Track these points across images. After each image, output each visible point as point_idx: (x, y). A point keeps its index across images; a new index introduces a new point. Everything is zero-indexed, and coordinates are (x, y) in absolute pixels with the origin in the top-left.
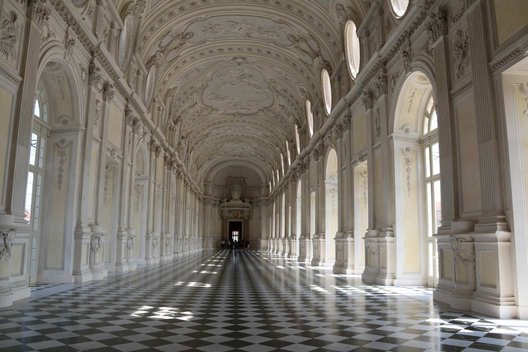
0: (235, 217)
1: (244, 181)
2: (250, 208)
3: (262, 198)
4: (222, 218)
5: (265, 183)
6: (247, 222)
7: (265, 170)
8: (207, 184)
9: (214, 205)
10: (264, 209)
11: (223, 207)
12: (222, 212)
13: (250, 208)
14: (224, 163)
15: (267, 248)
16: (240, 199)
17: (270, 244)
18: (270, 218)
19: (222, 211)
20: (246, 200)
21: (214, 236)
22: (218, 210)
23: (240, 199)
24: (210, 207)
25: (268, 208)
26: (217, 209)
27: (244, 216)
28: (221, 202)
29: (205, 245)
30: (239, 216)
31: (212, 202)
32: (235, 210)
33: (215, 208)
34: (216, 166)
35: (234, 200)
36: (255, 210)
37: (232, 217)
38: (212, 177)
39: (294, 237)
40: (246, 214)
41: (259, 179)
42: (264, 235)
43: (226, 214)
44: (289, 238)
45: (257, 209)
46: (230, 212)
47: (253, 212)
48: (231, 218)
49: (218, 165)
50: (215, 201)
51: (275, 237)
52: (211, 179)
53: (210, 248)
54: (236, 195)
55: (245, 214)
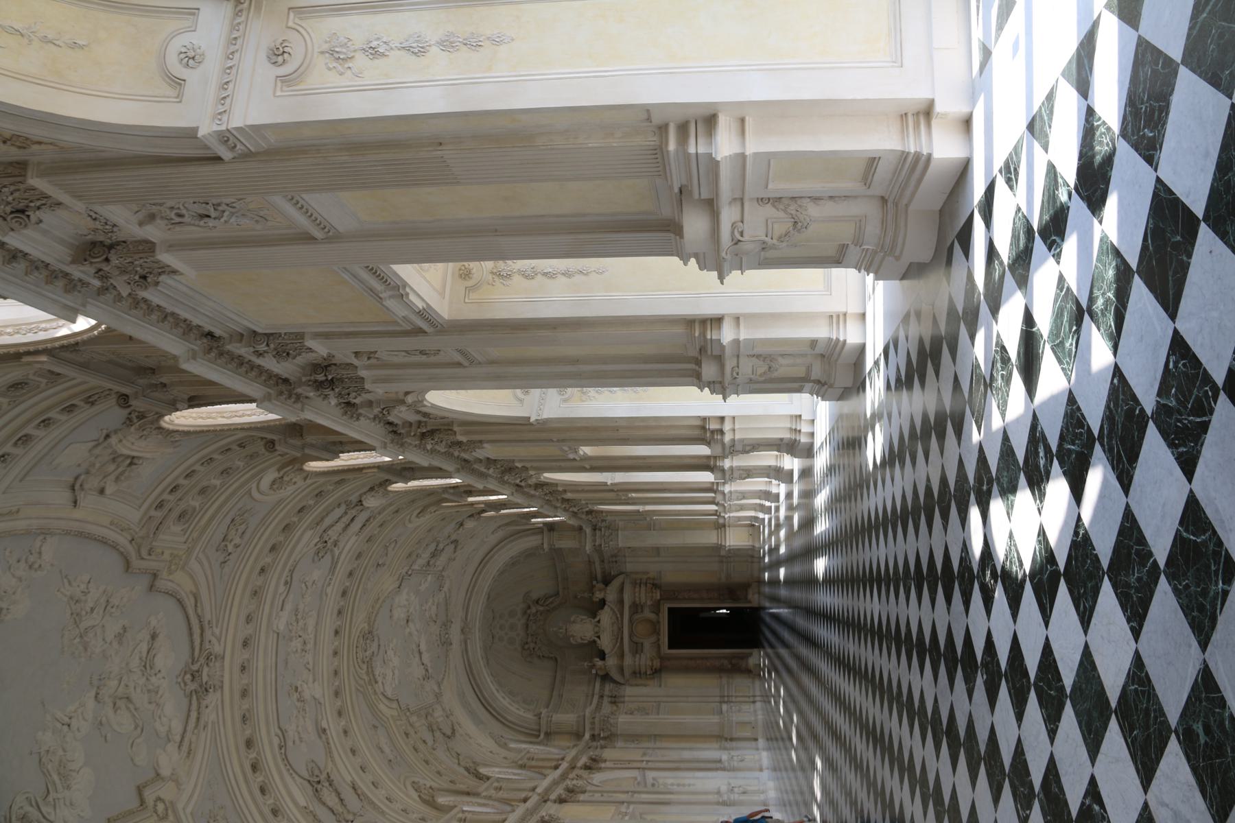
0: (656, 631)
1: (537, 602)
2: (623, 583)
3: (588, 547)
4: (657, 672)
5: (539, 537)
6: (670, 592)
7: (493, 539)
8: (544, 729)
9: (614, 703)
10: (623, 540)
11: (621, 670)
12: (636, 674)
13: (623, 583)
14: (475, 672)
15: (753, 525)
16: (594, 615)
17: (739, 518)
18: (651, 519)
19: (634, 673)
20: (598, 595)
21: (718, 699)
22: (632, 685)
23: (593, 614)
24: (622, 719)
25: (621, 524)
26: (629, 691)
27: (649, 603)
28: (606, 678)
29: (748, 734)
30: (652, 616)
31: (607, 708)
32: (631, 635)
33: (627, 699)
34: (485, 699)
35: (599, 637)
36: (629, 567)
37: (653, 639)
38: (521, 713)
39: (714, 426)
40: (644, 596)
41: (530, 554)
42: (711, 538)
43: (646, 659)
44: (718, 450)
45: (628, 559)
46: (637, 648)
47: (637, 573)
48: (657, 645)
49: (481, 692)
50: (602, 697)
51: (717, 504)
52: (529, 716)
53: (755, 711)
54: (582, 629)
55: (643, 600)
